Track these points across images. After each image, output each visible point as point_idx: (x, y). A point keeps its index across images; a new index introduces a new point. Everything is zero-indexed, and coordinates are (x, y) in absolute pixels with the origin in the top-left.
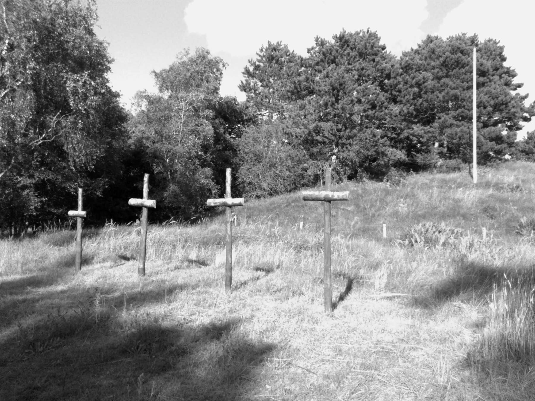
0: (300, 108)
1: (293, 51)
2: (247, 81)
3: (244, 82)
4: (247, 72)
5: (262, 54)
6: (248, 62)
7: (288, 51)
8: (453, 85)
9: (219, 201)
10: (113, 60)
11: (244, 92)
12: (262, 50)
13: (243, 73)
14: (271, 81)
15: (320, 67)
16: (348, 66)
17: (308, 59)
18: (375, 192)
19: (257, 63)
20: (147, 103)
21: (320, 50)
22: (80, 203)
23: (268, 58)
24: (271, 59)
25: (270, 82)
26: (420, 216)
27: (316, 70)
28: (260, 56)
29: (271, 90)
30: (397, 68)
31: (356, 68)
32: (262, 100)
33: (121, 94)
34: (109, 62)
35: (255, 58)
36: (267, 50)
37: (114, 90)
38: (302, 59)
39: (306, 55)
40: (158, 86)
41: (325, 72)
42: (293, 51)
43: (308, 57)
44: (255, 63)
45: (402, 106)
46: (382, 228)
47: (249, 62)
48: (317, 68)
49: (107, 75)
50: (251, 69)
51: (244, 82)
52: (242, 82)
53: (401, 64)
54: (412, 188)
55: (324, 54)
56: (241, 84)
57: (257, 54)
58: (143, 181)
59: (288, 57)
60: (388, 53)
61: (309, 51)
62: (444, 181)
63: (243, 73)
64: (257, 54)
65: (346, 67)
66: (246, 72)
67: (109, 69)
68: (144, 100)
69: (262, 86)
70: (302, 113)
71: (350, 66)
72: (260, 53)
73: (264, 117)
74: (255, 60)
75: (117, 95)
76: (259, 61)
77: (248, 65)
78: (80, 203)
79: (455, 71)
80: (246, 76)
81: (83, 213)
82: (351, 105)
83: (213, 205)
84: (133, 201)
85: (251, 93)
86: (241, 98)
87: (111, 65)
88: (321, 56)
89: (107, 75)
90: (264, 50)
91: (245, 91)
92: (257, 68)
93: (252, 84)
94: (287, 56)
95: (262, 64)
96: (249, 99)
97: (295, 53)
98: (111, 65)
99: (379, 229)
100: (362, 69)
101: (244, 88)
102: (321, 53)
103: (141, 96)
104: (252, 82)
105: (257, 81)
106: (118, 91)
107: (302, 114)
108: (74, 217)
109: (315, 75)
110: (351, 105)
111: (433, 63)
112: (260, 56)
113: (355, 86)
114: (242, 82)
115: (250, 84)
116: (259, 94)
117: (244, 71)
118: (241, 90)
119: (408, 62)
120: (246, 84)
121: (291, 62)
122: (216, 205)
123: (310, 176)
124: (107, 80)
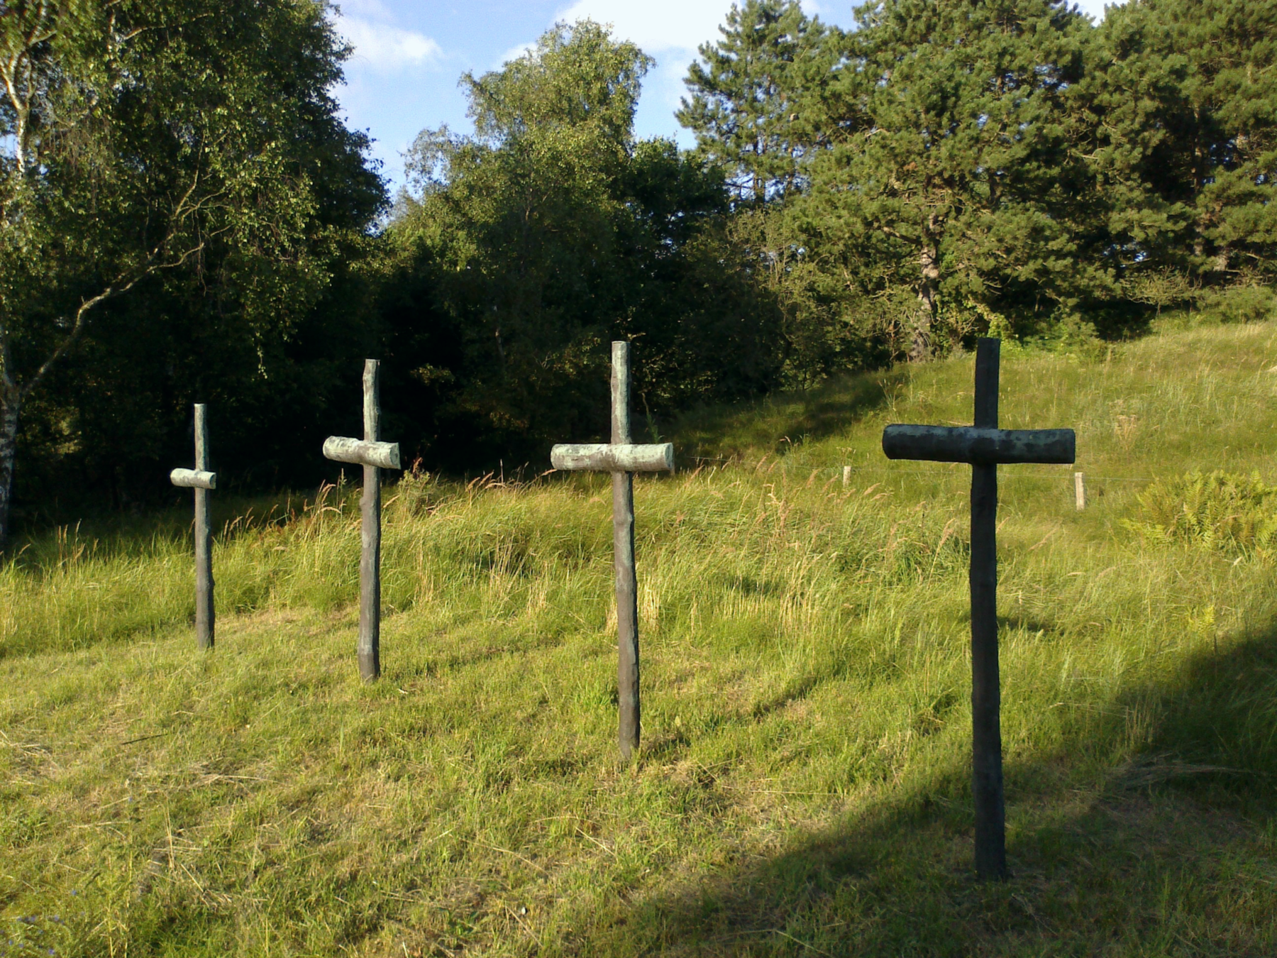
0: (839, 161)
1: (816, 18)
2: (697, 99)
3: (691, 101)
4: (697, 78)
5: (732, 30)
6: (698, 52)
7: (803, 18)
8: (1254, 88)
9: (591, 452)
10: (349, 49)
11: (690, 130)
12: (732, 20)
13: (688, 81)
14: (760, 95)
15: (889, 56)
16: (963, 50)
17: (859, 34)
18: (1040, 381)
19: (722, 52)
20: (448, 163)
21: (888, 8)
22: (200, 445)
23: (749, 37)
24: (756, 39)
25: (755, 99)
26: (1171, 445)
27: (879, 65)
28: (728, 34)
29: (760, 121)
30: (1100, 48)
31: (985, 52)
32: (738, 146)
33: (370, 138)
34: (340, 56)
35: (716, 39)
36: (745, 16)
37: (351, 128)
38: (842, 36)
39: (850, 25)
40: (475, 118)
41: (902, 66)
42: (816, 18)
43: (855, 30)
44: (717, 53)
45: (1109, 149)
46: (1073, 482)
47: (703, 51)
48: (880, 56)
49: (334, 91)
50: (707, 69)
51: (691, 101)
52: (684, 102)
53: (1107, 37)
54: (1141, 368)
55: (901, 19)
56: (682, 108)
57: (722, 30)
58: (361, 383)
59: (801, 35)
60: (1070, 7)
61: (858, 12)
62: (1225, 347)
63: (688, 81)
64: (722, 30)
65: (957, 53)
66: (695, 78)
67: (336, 75)
68: (440, 154)
69: (733, 111)
70: (843, 174)
71: (969, 50)
72: (728, 28)
73: (744, 191)
74: (715, 46)
75: (361, 141)
76: (730, 49)
77: (700, 59)
78: (200, 445)
79: (1255, 48)
80: (696, 87)
81: (206, 476)
82: (975, 149)
83: (569, 464)
84: (334, 447)
85: (708, 130)
86: (687, 141)
87: (344, 65)
88: (893, 25)
89: (334, 91)
90: (738, 19)
91: (695, 127)
92: (723, 63)
93: (710, 107)
94: (800, 31)
95: (733, 56)
96: (704, 146)
97: (821, 21)
98: (344, 65)
99: (1064, 485)
100: (1002, 54)
101: (694, 117)
102: (892, 16)
103: (430, 144)
104: (711, 100)
105: (723, 98)
106: (363, 131)
107: (845, 177)
108: (187, 492)
109: (877, 77)
110: (975, 149)
111: (1194, 30)
112: (728, 34)
113: (983, 100)
114: (684, 102)
115: (705, 106)
116: (730, 131)
117: (687, 74)
118: (685, 126)
119: (1131, 30)
120: (695, 107)
121: (812, 46)
122: (581, 464)
123: (865, 340)
124: (333, 101)
